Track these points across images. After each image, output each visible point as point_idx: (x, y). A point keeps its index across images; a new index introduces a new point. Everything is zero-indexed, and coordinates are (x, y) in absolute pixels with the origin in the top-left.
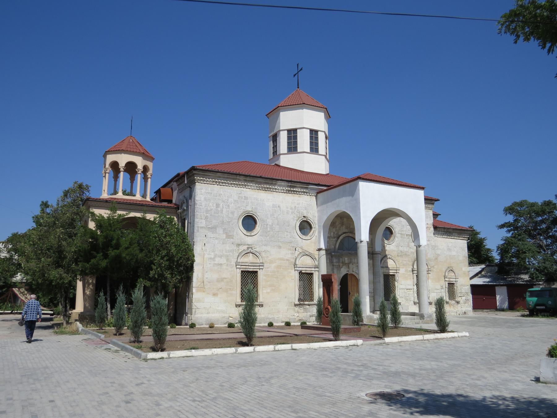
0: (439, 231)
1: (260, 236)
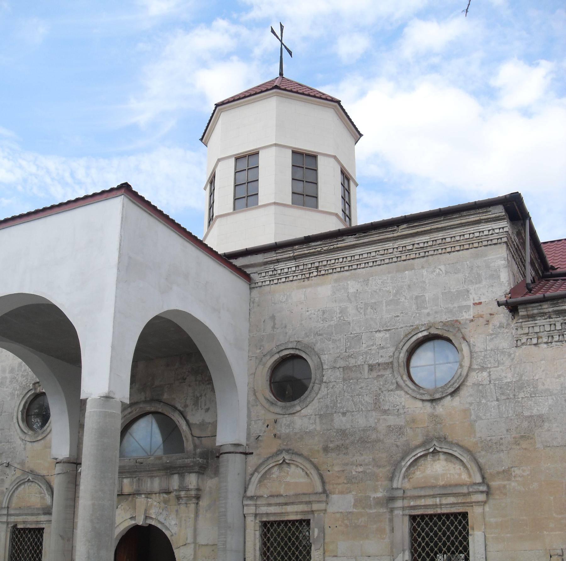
0: (532, 317)
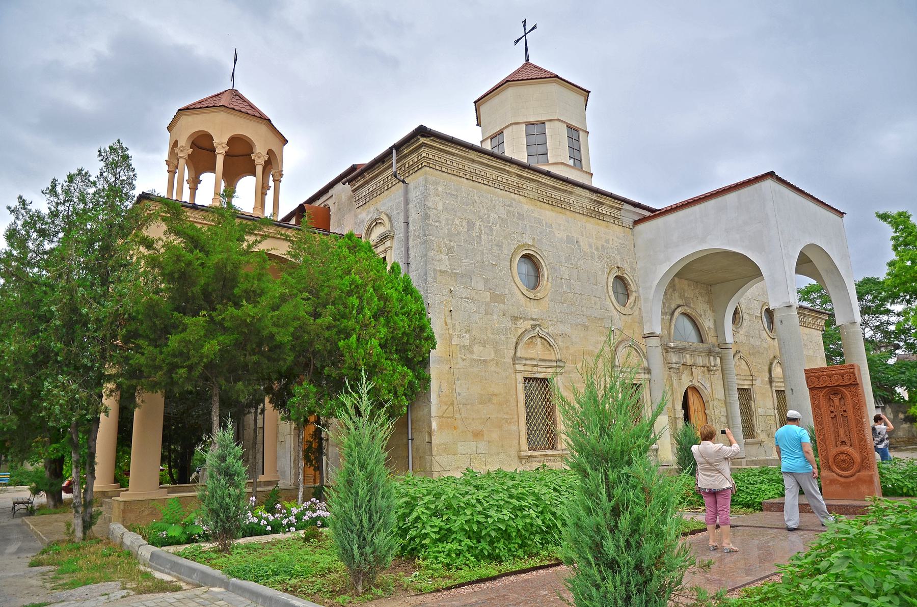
1: (552, 300)
